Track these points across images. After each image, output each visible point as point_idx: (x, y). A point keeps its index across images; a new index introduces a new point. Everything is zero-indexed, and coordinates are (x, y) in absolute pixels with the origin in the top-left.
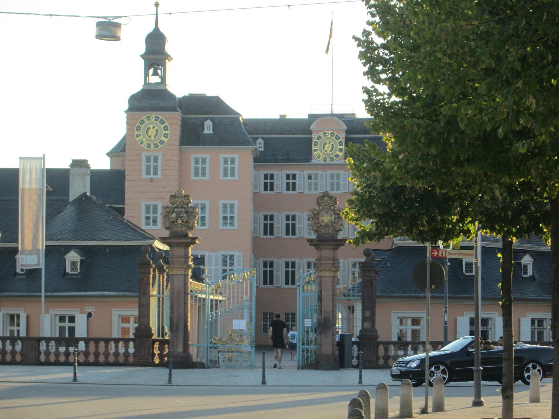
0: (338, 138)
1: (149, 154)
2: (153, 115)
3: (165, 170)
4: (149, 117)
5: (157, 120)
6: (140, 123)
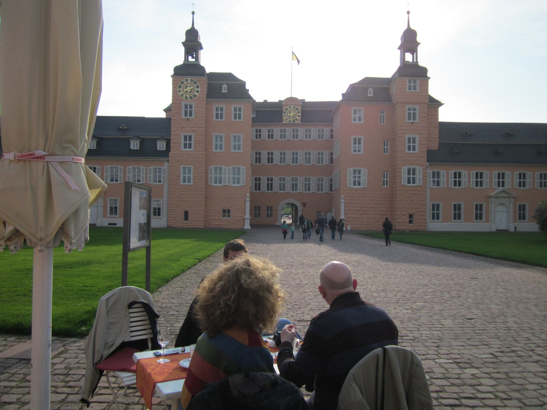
0: (297, 109)
1: (186, 103)
2: (189, 79)
3: (196, 113)
4: (187, 79)
5: (192, 82)
6: (181, 83)
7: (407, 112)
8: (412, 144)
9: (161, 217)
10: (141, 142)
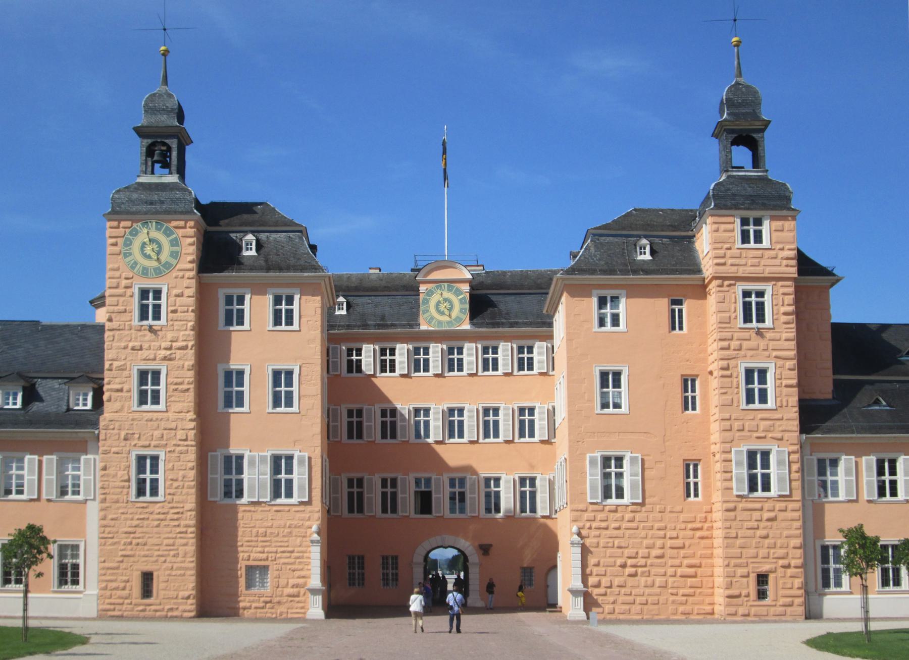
3: (175, 311)
6: (131, 234)
7: (740, 300)
8: (756, 386)
9: (80, 587)
10: (25, 390)
